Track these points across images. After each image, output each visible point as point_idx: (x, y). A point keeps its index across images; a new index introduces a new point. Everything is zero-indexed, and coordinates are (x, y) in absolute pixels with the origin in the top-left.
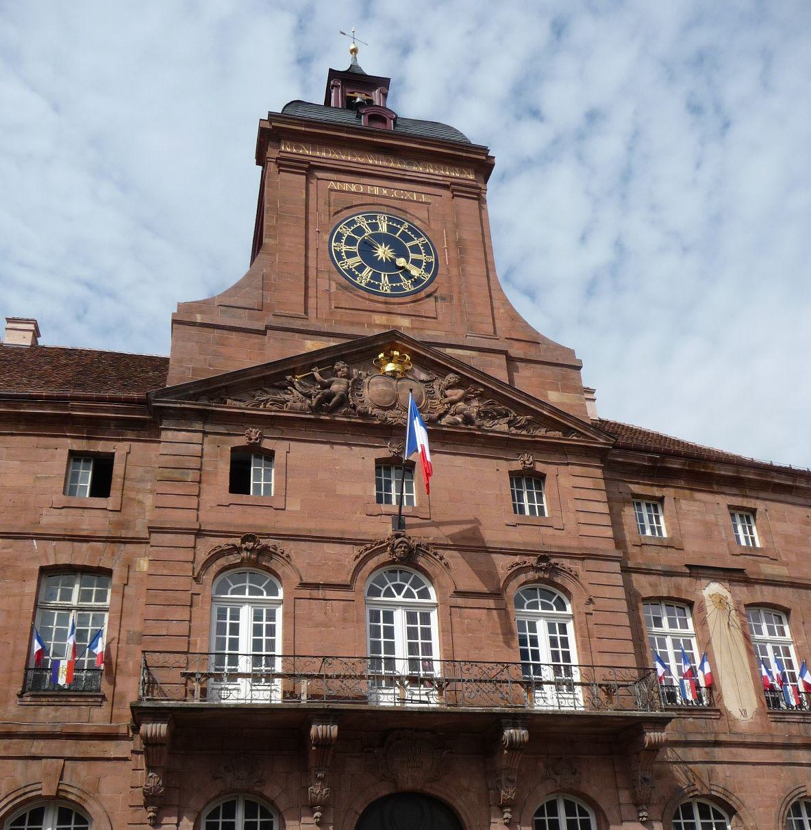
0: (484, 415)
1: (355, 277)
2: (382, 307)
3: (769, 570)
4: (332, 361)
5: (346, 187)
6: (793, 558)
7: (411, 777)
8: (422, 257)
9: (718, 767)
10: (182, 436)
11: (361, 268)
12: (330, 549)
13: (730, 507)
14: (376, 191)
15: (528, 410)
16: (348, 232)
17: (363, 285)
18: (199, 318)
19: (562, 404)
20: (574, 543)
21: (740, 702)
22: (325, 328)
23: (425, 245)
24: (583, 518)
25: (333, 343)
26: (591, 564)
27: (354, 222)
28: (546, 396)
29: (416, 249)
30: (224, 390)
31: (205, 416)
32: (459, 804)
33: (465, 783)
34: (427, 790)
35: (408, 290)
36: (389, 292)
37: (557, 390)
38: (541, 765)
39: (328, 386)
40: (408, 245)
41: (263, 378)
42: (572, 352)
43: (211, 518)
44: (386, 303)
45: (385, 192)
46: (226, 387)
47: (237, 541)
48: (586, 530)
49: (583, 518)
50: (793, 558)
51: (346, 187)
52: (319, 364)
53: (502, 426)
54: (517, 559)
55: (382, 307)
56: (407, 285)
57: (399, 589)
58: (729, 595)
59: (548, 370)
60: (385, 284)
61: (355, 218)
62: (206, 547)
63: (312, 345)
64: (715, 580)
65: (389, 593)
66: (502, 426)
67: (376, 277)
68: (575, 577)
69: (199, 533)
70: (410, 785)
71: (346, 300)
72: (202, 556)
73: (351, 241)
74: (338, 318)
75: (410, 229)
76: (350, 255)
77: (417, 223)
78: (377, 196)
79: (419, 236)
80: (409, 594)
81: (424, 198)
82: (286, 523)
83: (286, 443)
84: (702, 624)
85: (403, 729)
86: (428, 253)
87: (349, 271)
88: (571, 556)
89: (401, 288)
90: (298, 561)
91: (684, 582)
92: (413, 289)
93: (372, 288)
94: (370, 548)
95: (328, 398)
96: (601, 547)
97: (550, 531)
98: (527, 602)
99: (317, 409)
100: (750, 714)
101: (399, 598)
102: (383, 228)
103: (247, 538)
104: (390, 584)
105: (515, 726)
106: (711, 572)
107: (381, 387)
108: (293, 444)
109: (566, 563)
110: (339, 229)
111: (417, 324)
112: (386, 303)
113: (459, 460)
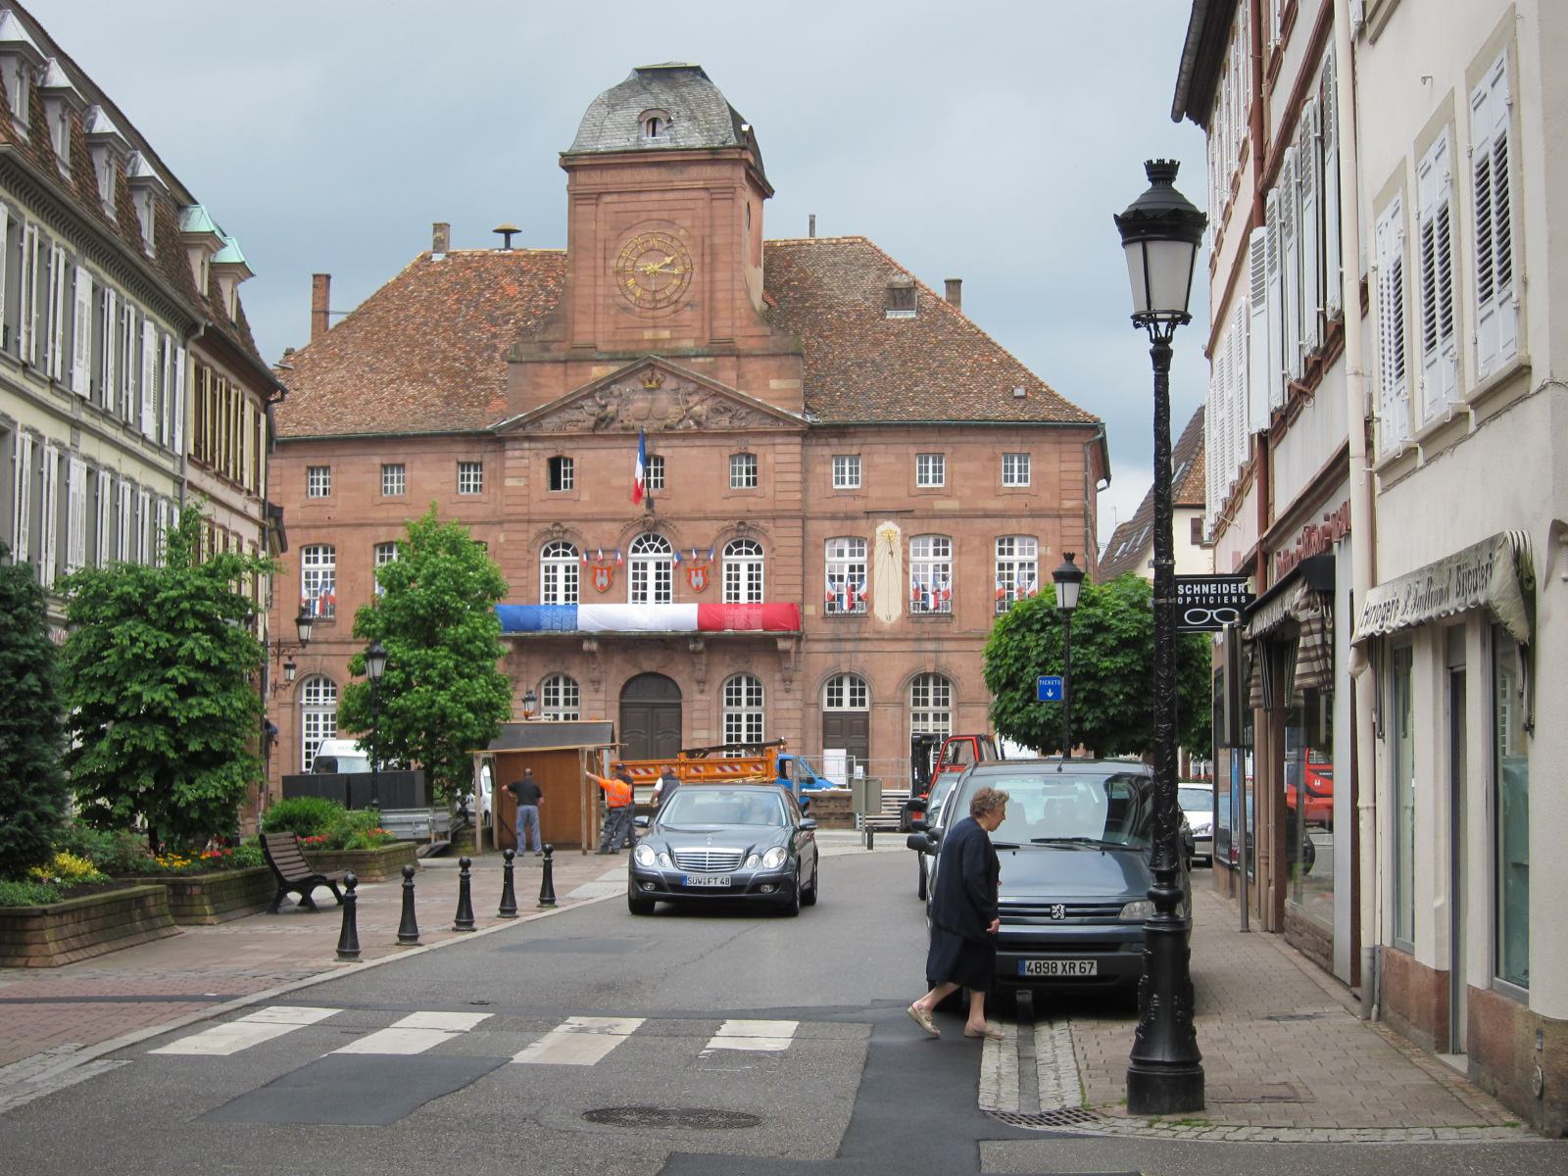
0: (716, 411)
3: (940, 505)
4: (607, 387)
6: (968, 492)
7: (649, 665)
9: (861, 655)
10: (517, 453)
12: (607, 526)
15: (748, 406)
20: (770, 507)
21: (888, 608)
24: (779, 487)
25: (613, 369)
26: (779, 522)
31: (530, 438)
32: (678, 680)
33: (681, 668)
39: (605, 406)
43: (537, 508)
47: (549, 526)
48: (781, 496)
49: (779, 487)
50: (968, 492)
53: (724, 421)
54: (727, 523)
57: (651, 547)
58: (899, 530)
62: (534, 529)
63: (598, 372)
64: (888, 519)
65: (645, 551)
66: (724, 421)
68: (764, 532)
69: (529, 521)
70: (648, 670)
72: (532, 536)
80: (658, 550)
81: (690, 204)
82: (579, 510)
83: (580, 452)
84: (871, 554)
88: (766, 518)
90: (588, 536)
91: (863, 523)
94: (629, 522)
95: (602, 420)
97: (753, 500)
99: (596, 425)
100: (894, 619)
101: (651, 554)
103: (557, 524)
107: (640, 404)
108: (585, 452)
109: (762, 523)
111: (675, 335)
113: (694, 451)
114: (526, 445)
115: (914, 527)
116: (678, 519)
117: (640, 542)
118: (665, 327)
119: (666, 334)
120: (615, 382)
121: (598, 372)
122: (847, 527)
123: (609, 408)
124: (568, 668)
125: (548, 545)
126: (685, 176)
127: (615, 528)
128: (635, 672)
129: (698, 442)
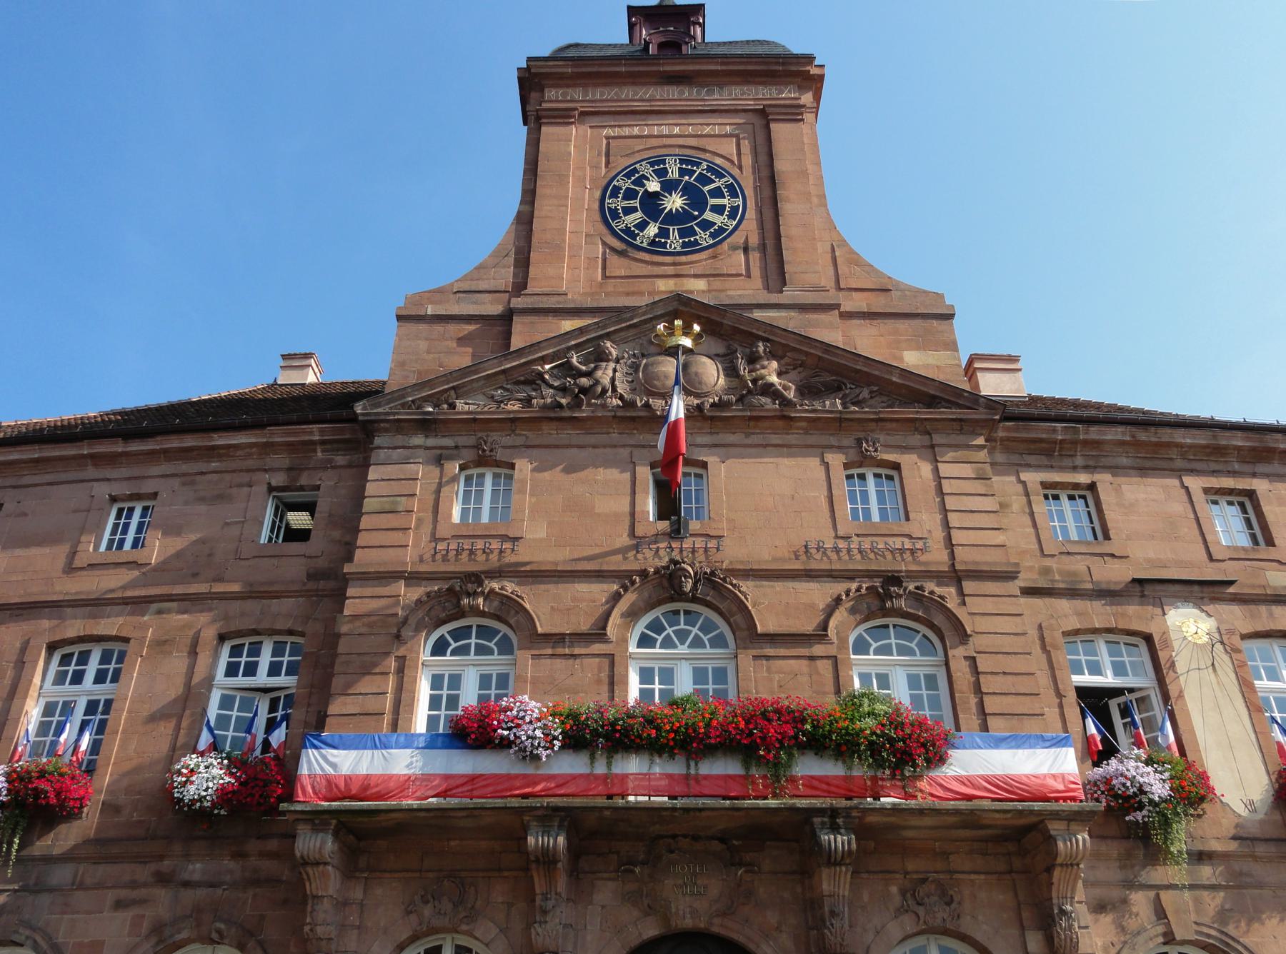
1: (634, 236)
2: (670, 270)
5: (626, 131)
8: (725, 201)
11: (642, 226)
12: (584, 589)
13: (1207, 491)
14: (665, 130)
16: (627, 184)
17: (644, 245)
18: (430, 310)
19: (926, 366)
22: (589, 303)
23: (731, 188)
27: (636, 171)
28: (901, 359)
29: (717, 193)
30: (452, 393)
34: (715, 929)
35: (705, 244)
36: (679, 249)
37: (918, 348)
38: (894, 889)
40: (706, 189)
41: (504, 372)
42: (940, 296)
44: (674, 264)
45: (677, 130)
46: (453, 388)
51: (626, 131)
52: (578, 347)
55: (670, 270)
56: (704, 238)
57: (682, 635)
59: (902, 325)
60: (674, 240)
61: (637, 166)
64: (1186, 599)
65: (667, 643)
67: (663, 233)
70: (688, 923)
71: (619, 266)
73: (630, 194)
74: (610, 289)
75: (709, 169)
76: (629, 211)
77: (719, 161)
78: (667, 136)
79: (721, 176)
80: (697, 643)
85: (674, 837)
86: (734, 194)
87: (627, 231)
88: (939, 577)
89: (696, 243)
92: (711, 242)
93: (656, 246)
96: (989, 559)
98: (874, 645)
101: (683, 649)
102: (674, 173)
104: (669, 630)
105: (835, 829)
106: (1177, 587)
110: (615, 182)
112: (674, 264)
114: (418, 440)
115: (1237, 617)
116: (749, 574)
117: (656, 627)
118: (696, 276)
119: (701, 285)
120: (608, 336)
121: (568, 325)
122: (1099, 613)
123: (599, 373)
124: (472, 917)
125: (443, 630)
126: (725, 94)
127: (599, 592)
128: (651, 930)
129: (775, 439)
